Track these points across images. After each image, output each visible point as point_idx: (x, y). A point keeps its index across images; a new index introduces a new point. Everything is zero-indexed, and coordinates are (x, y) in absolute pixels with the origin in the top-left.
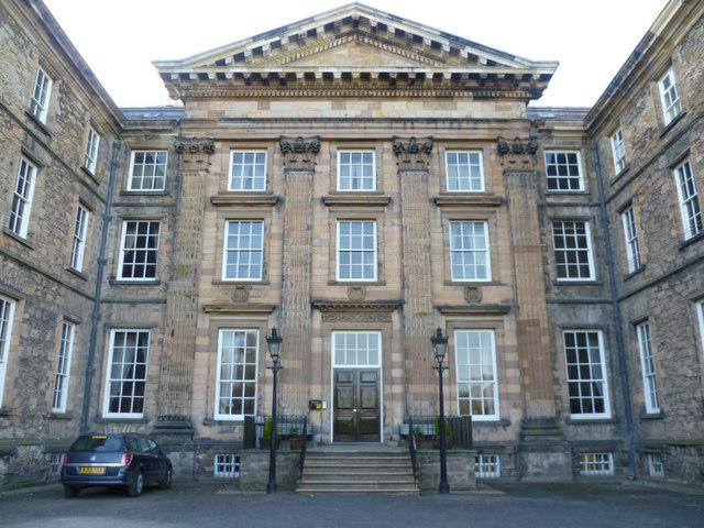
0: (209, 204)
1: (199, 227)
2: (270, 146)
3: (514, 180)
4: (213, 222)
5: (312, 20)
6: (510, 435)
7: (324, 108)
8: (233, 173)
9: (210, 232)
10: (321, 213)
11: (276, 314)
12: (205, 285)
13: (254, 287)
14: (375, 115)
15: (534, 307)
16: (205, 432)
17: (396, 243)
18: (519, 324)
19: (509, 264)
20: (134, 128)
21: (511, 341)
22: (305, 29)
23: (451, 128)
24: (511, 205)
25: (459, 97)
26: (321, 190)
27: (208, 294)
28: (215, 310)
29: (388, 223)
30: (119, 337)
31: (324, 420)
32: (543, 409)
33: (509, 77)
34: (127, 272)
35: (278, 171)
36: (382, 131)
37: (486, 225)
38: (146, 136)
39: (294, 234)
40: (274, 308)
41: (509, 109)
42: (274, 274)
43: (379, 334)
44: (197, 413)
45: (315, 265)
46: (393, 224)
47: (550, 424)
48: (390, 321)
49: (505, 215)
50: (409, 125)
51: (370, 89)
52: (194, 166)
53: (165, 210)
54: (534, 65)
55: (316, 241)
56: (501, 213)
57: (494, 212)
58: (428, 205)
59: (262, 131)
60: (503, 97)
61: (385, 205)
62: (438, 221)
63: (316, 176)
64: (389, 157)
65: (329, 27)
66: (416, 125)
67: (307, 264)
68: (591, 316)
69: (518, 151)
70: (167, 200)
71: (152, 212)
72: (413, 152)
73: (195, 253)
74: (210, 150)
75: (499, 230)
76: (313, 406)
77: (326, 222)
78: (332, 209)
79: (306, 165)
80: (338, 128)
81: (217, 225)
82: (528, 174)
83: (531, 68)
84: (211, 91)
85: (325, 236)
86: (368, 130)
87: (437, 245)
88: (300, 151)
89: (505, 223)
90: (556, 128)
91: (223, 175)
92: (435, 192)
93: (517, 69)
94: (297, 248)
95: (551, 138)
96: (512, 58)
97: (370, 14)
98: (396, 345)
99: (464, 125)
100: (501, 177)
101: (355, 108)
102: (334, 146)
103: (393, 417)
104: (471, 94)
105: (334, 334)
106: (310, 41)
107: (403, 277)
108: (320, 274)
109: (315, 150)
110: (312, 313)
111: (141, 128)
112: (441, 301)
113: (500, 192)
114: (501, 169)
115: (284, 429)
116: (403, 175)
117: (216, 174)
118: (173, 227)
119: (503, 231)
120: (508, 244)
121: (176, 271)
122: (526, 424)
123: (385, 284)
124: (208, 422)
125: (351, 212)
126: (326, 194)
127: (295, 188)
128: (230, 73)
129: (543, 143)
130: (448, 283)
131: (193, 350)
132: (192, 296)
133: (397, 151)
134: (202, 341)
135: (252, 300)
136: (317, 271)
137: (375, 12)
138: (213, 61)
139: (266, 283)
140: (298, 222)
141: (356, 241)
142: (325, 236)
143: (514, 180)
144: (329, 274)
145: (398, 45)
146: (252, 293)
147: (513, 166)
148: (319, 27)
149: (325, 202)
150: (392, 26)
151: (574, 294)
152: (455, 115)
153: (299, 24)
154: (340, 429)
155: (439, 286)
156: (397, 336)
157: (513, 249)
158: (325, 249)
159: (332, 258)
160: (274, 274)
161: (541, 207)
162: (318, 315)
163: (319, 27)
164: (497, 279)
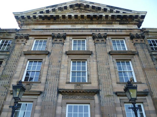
0: (23, 54)
1: (17, 62)
2: (49, 38)
3: (138, 46)
4: (23, 60)
5: (65, 3)
8: (33, 45)
9: (21, 64)
10: (65, 58)
11: (41, 96)
13: (34, 84)
17: (95, 68)
18: (153, 100)
19: (143, 75)
20: (3, 31)
22: (63, 6)
23: (113, 32)
24: (139, 54)
25: (114, 23)
26: (66, 49)
29: (91, 61)
33: (131, 16)
35: (50, 45)
36: (88, 32)
37: (130, 62)
38: (7, 35)
39: (54, 64)
40: (41, 93)
41: (132, 27)
42: (43, 79)
43: (89, 106)
45: (61, 75)
46: (93, 61)
48: (94, 99)
49: (137, 58)
50: (98, 31)
51: (84, 21)
52: (20, 42)
53: (6, 56)
54: (139, 13)
55: (62, 67)
56: (136, 57)
57: (133, 57)
58: (107, 55)
59: (46, 33)
60: (129, 24)
61: (90, 54)
62: (112, 60)
63: (64, 46)
65: (71, 6)
66: (100, 31)
67: (58, 75)
69: (138, 37)
70: (8, 53)
74: (27, 38)
75: (136, 63)
77: (67, 60)
78: (69, 56)
79: (61, 42)
80: (72, 32)
81: (24, 61)
82: (143, 44)
83: (138, 13)
84: (32, 22)
85: (66, 65)
86: (83, 32)
89: (138, 60)
90: (150, 31)
94: (54, 69)
95: (148, 35)
96: (131, 11)
97: (84, 2)
98: (97, 111)
99: (117, 31)
100: (133, 46)
102: (71, 38)
104: (118, 22)
105: (68, 105)
106: (65, 10)
107: (99, 80)
108: (63, 80)
109: (64, 37)
110: (58, 95)
111: (5, 31)
112: (116, 90)
113: (134, 50)
114: (133, 44)
116: (97, 45)
117: (28, 46)
118: (7, 63)
119: (138, 63)
120: (141, 68)
123: (91, 83)
125: (77, 57)
126: (67, 50)
128: (37, 16)
129: (146, 37)
135: (32, 89)
136: (62, 78)
137: (86, 2)
138: (33, 13)
140: (56, 60)
141: (79, 68)
142: (66, 65)
144: (67, 79)
145: (93, 11)
146: (33, 86)
147: (137, 42)
148: (68, 6)
149: (67, 54)
150: (91, 5)
153: (62, 4)
155: (115, 84)
156: (97, 106)
157: (144, 70)
158: (66, 70)
159: (68, 73)
160: (43, 79)
162: (60, 96)
163: (68, 6)
164: (139, 81)
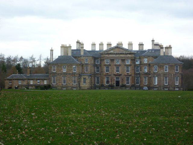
6: (130, 86)
7: (114, 56)
12: (104, 73)
14: (119, 56)
15: (133, 75)
16: (105, 86)
21: (131, 78)
26: (114, 64)
27: (104, 74)
28: (105, 75)
30: (97, 78)
31: (115, 85)
32: (133, 84)
34: (97, 72)
35: (110, 62)
44: (104, 84)
47: (134, 85)
56: (131, 66)
64: (121, 60)
67: (113, 71)
68: (138, 76)
69: (133, 60)
71: (99, 66)
72: (123, 60)
73: (103, 70)
76: (114, 83)
87: (125, 69)
88: (112, 60)
91: (105, 62)
92: (125, 64)
93: (133, 52)
101: (117, 56)
103: (121, 84)
108: (114, 72)
109: (114, 60)
113: (131, 64)
115: (112, 85)
121: (101, 72)
122: (132, 85)
124: (105, 85)
127: (112, 64)
130: (126, 73)
131: (103, 79)
132: (103, 74)
133: (122, 60)
134: (104, 78)
139: (110, 73)
143: (133, 63)
151: (137, 74)
152: (127, 56)
154: (116, 85)
161: (135, 66)
